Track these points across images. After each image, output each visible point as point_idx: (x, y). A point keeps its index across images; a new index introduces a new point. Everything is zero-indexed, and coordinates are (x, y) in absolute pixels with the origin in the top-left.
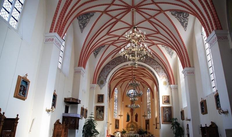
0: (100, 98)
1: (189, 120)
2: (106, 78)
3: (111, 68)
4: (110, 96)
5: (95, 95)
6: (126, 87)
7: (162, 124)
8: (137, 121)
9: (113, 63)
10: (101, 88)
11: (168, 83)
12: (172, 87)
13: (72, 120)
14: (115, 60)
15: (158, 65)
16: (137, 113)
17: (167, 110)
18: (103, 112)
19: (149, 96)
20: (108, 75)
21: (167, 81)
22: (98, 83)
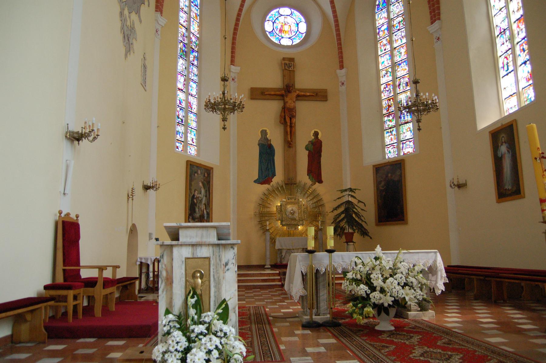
8: (320, 181)
16: (316, 134)
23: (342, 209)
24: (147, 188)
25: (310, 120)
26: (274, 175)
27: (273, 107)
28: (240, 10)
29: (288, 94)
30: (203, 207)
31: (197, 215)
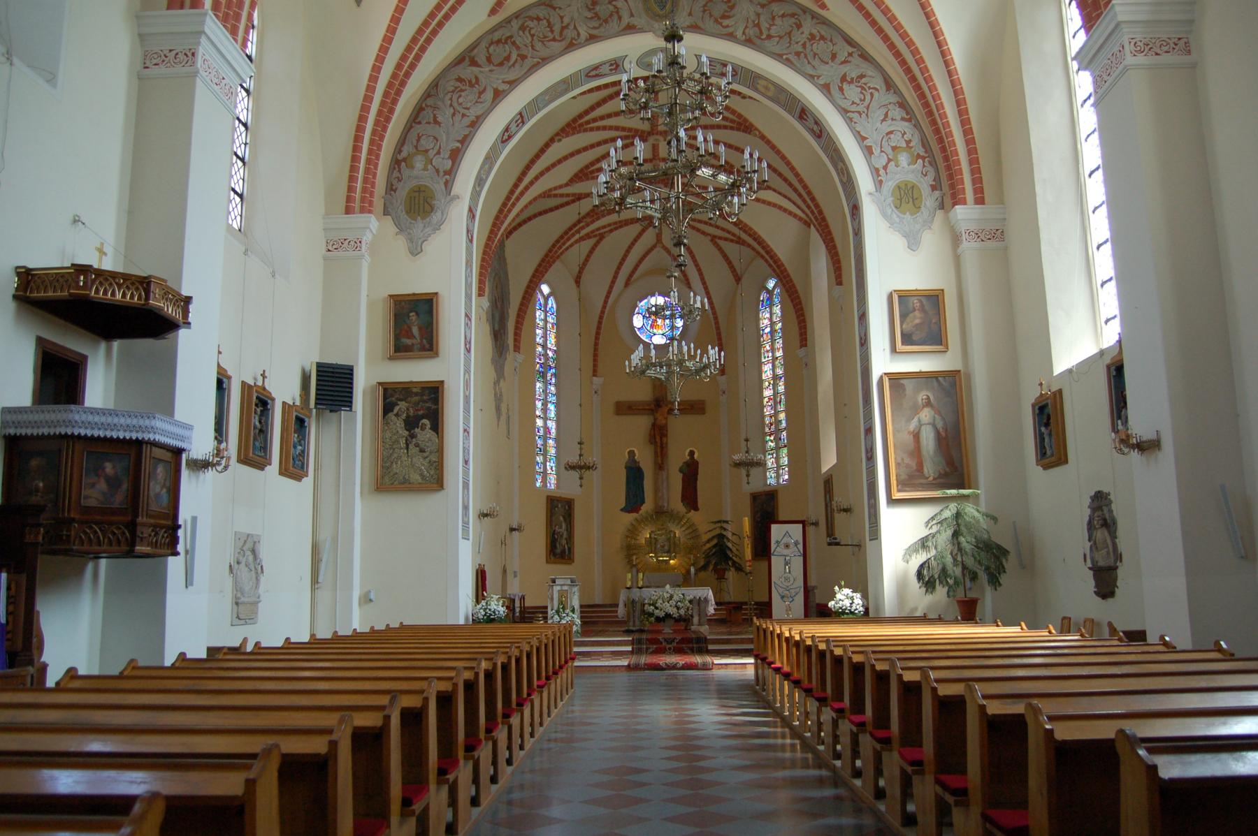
0: (413, 323)
1: (1147, 447)
2: (450, 162)
3: (489, 95)
4: (498, 335)
5: (371, 305)
6: (617, 273)
7: (892, 502)
8: (696, 509)
9: (499, 52)
10: (415, 250)
11: (929, 200)
12: (962, 227)
13: (98, 470)
14: (515, 25)
15: (856, 60)
16: (692, 453)
17: (922, 396)
18: (437, 426)
19: (773, 332)
20: (465, 140)
21: (924, 185)
22: (386, 213)
23: (715, 541)
24: (512, 530)
25: (684, 438)
26: (643, 502)
27: (642, 423)
28: (603, 312)
29: (657, 408)
30: (564, 542)
31: (558, 551)
